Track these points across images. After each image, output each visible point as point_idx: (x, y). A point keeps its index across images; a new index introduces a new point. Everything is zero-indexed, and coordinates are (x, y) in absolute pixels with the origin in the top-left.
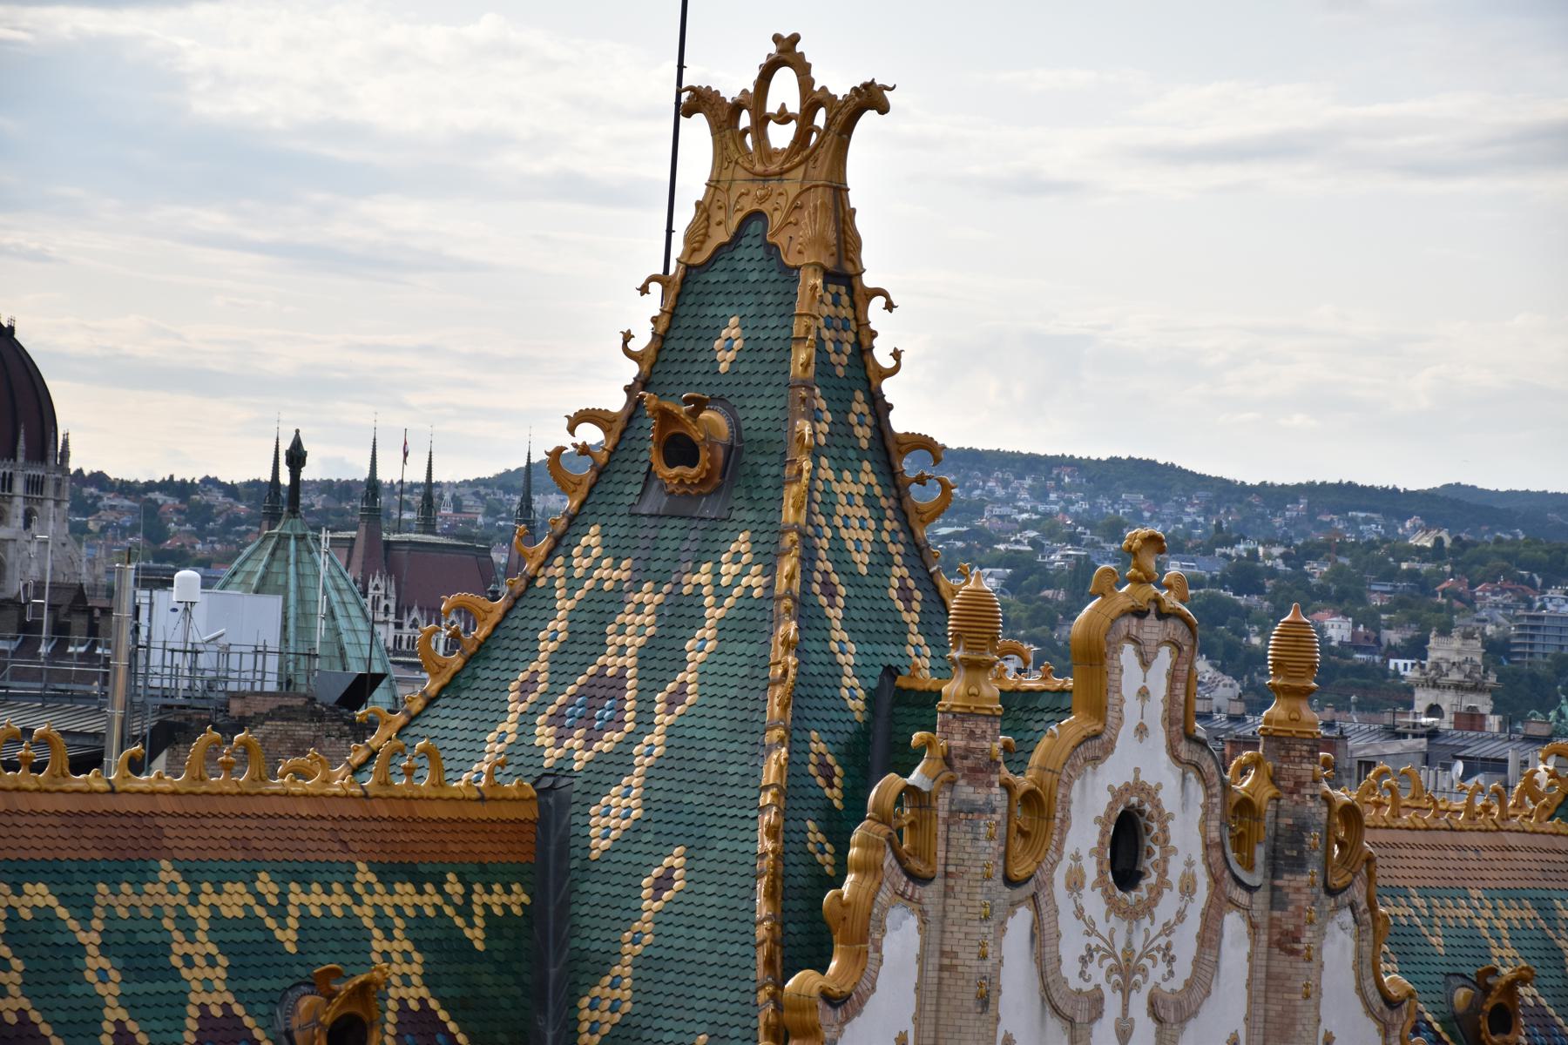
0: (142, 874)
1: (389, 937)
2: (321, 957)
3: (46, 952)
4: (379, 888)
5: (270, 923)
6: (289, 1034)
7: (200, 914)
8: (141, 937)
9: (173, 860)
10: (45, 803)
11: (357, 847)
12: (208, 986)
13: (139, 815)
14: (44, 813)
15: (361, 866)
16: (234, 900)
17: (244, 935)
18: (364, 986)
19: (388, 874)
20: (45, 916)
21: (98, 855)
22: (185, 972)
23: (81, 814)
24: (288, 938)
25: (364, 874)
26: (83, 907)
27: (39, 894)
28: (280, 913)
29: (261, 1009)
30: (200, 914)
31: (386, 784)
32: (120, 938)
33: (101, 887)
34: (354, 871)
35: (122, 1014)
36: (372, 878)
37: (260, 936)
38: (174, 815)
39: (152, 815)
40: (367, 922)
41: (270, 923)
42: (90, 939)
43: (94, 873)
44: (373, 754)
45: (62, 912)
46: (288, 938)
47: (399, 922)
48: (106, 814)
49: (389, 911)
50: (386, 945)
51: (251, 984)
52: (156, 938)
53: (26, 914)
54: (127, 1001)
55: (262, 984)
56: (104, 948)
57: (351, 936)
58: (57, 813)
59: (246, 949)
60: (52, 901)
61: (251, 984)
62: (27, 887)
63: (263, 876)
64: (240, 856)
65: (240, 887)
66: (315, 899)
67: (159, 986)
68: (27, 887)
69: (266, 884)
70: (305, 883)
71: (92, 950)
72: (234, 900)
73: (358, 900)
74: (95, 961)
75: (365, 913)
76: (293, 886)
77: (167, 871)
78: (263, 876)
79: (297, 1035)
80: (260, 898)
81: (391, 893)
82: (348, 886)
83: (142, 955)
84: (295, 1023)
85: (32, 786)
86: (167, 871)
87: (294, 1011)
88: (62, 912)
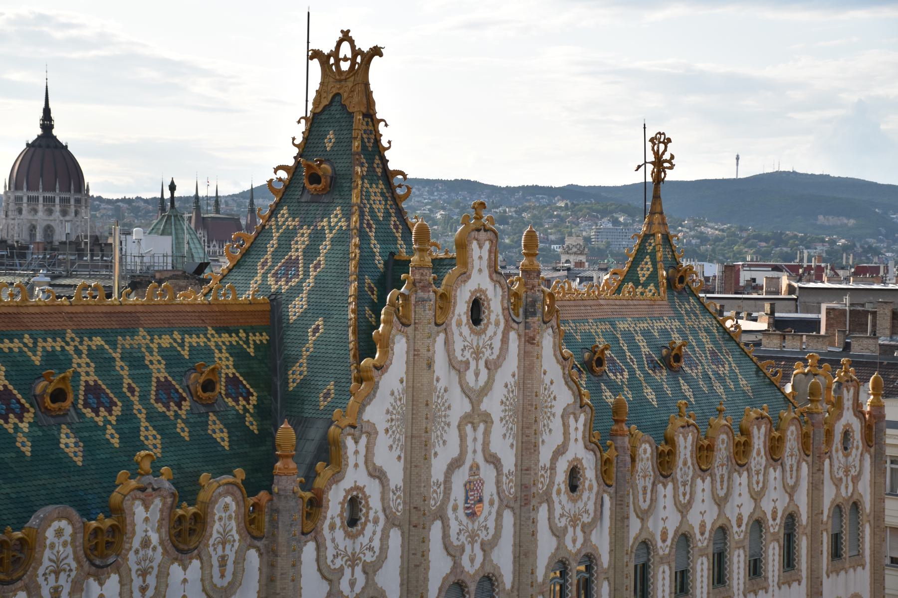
0: (133, 333)
1: (221, 352)
2: (197, 360)
3: (102, 361)
4: (216, 335)
5: (179, 349)
6: (188, 386)
7: (154, 346)
8: (135, 355)
9: (144, 328)
10: (98, 309)
11: (208, 321)
12: (159, 371)
13: (131, 313)
14: (98, 313)
15: (210, 328)
16: (166, 341)
17: (170, 353)
18: (213, 370)
19: (219, 331)
20: (101, 348)
21: (118, 327)
22: (150, 366)
23: (111, 313)
24: (185, 353)
25: (211, 331)
26: (114, 345)
27: (98, 341)
28: (182, 345)
29: (177, 378)
30: (154, 346)
31: (217, 299)
32: (127, 355)
33: (120, 338)
34: (207, 330)
35: (130, 381)
36: (213, 332)
37: (176, 353)
38: (143, 312)
39: (135, 312)
40: (213, 348)
41: (179, 349)
42: (117, 355)
43: (117, 333)
44: (211, 290)
45: (107, 347)
46: (185, 353)
47: (224, 347)
48: (119, 312)
49: (220, 343)
50: (220, 355)
51: (174, 370)
52: (140, 355)
53: (94, 348)
54: (131, 376)
55: (178, 369)
56: (122, 359)
57: (207, 353)
58: (102, 313)
59: (171, 358)
60: (103, 343)
61: (174, 370)
62: (94, 338)
63: (175, 332)
64: (167, 326)
65: (168, 336)
66: (194, 340)
67: (142, 371)
68: (94, 338)
69: (176, 335)
70: (190, 335)
71: (118, 359)
72: (166, 341)
73: (209, 340)
74: (119, 363)
75: (212, 344)
76: (186, 336)
77: (142, 332)
78: (175, 332)
79: (191, 387)
80: (175, 340)
81: (221, 337)
82: (205, 335)
83: (135, 361)
84: (190, 382)
85: (93, 303)
86: (142, 332)
87: (189, 378)
88: (107, 347)
